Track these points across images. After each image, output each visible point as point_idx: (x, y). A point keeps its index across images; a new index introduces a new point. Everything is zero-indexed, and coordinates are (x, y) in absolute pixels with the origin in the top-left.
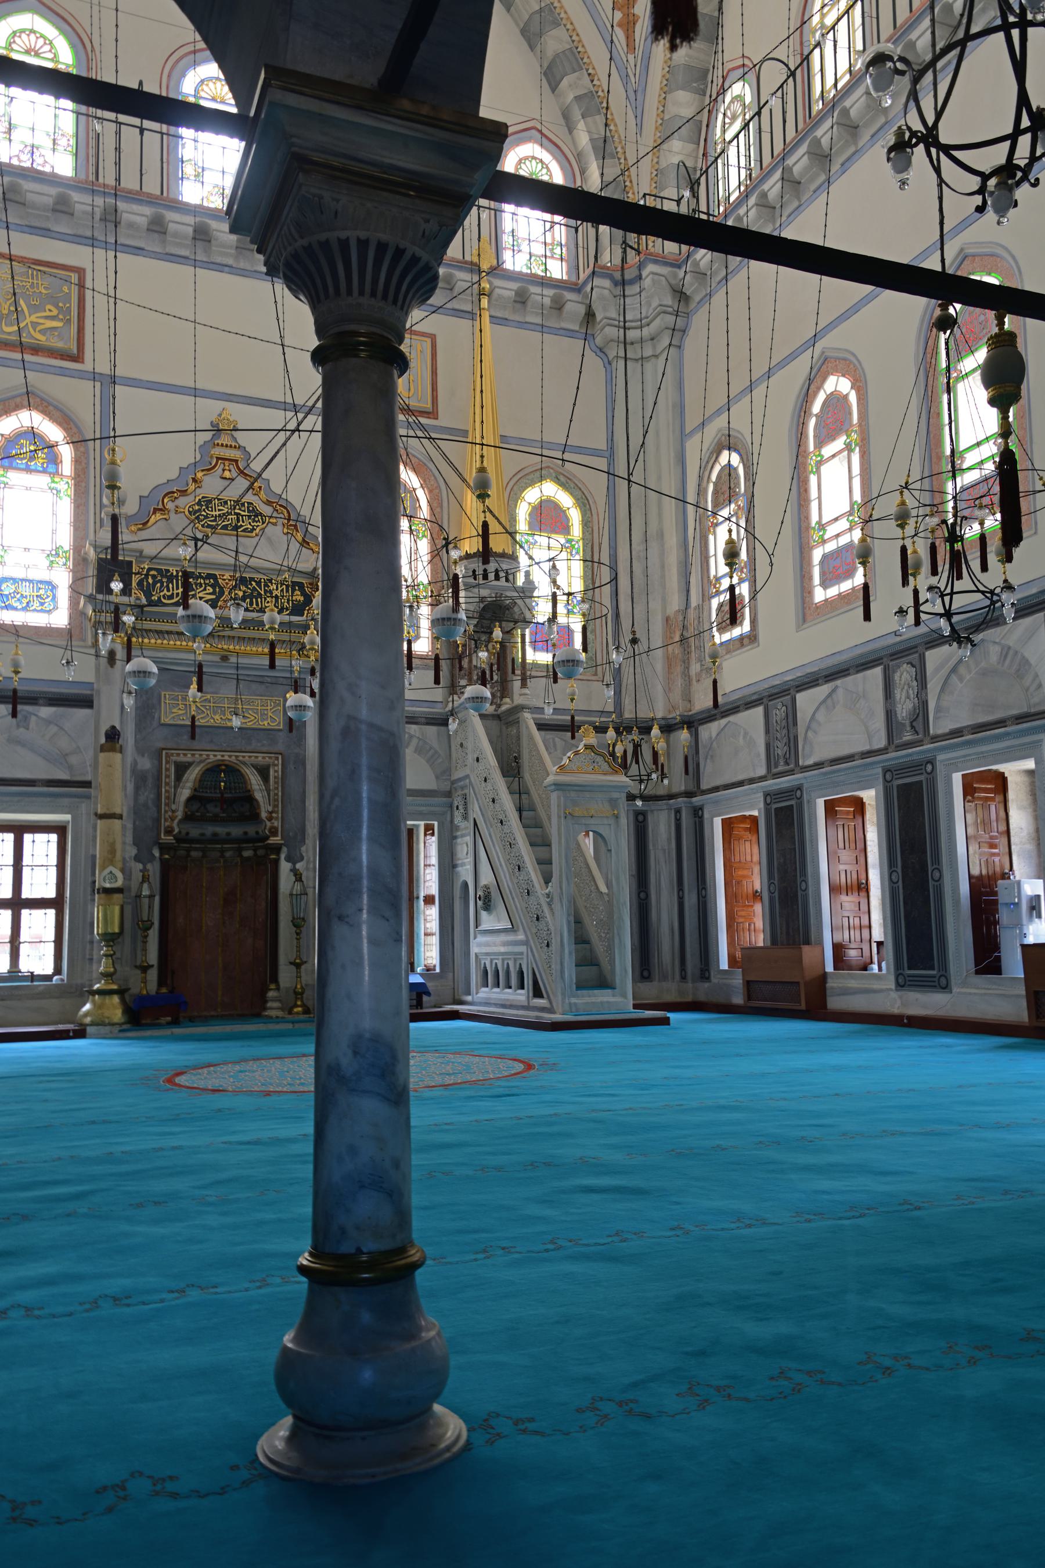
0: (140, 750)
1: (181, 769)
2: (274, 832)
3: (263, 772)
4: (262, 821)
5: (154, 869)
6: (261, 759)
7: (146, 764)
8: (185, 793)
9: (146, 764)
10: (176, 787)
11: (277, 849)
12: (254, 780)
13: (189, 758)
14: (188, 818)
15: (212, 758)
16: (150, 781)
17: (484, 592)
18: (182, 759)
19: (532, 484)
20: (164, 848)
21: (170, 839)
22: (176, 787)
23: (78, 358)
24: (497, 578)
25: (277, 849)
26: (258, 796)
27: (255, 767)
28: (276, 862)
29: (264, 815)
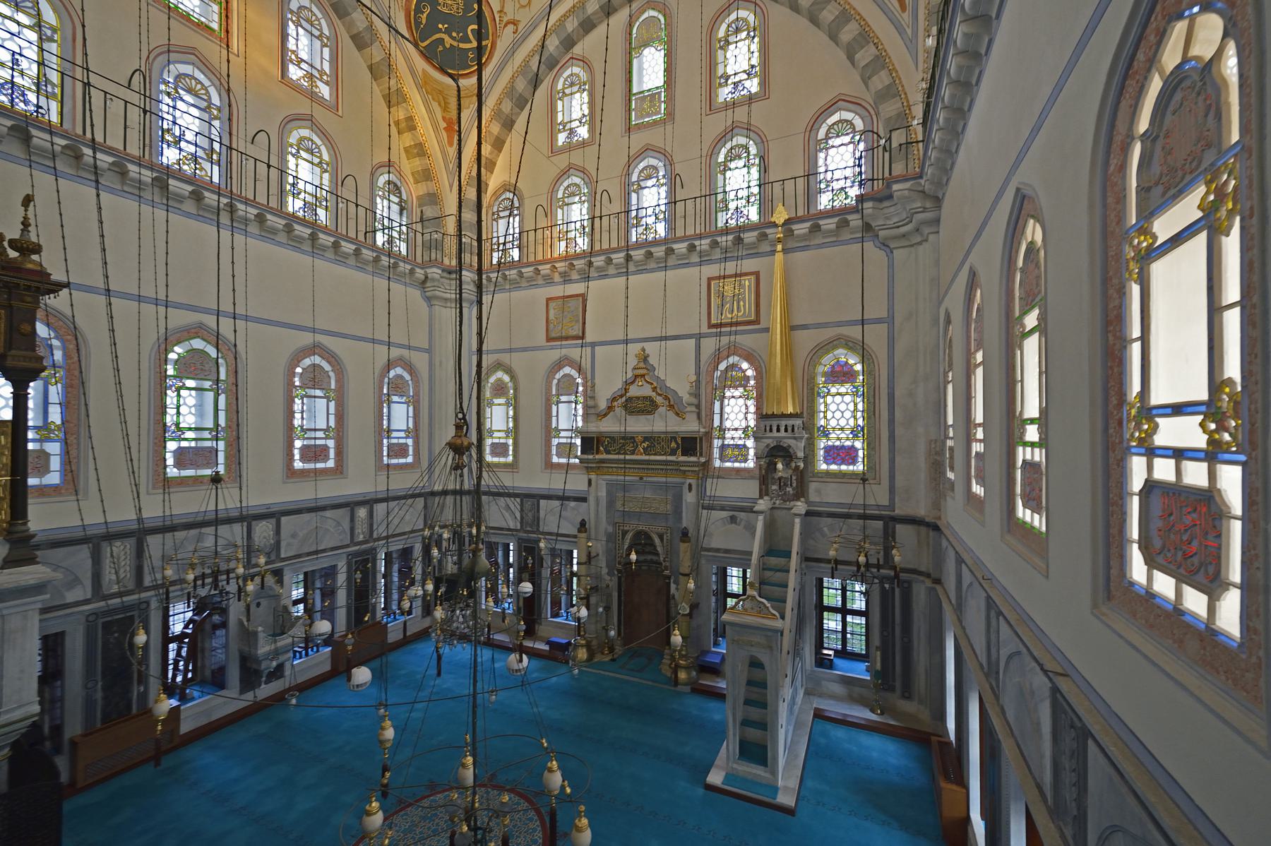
0: (608, 523)
1: (625, 533)
2: (666, 568)
5: (615, 579)
6: (660, 530)
7: (610, 529)
9: (610, 529)
11: (669, 578)
12: (657, 541)
17: (769, 441)
19: (827, 352)
20: (619, 571)
21: (620, 567)
23: (583, 337)
24: (778, 430)
26: (659, 549)
28: (669, 584)
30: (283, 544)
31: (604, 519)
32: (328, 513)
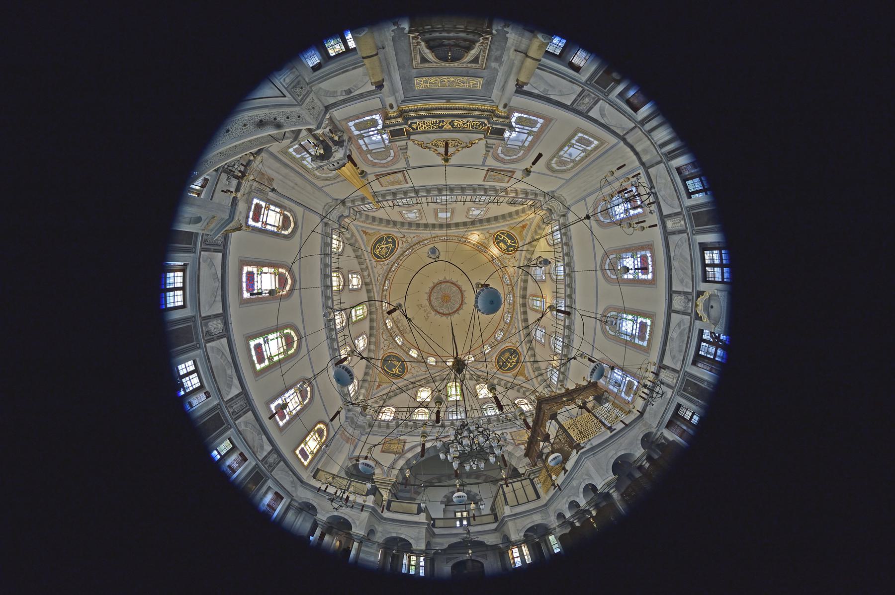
3: (424, 60)
4: (423, 40)
6: (426, 65)
8: (473, 52)
10: (479, 54)
12: (430, 55)
13: (469, 65)
14: (473, 42)
15: (456, 65)
16: (493, 58)
18: (474, 65)
22: (479, 54)
25: (410, 32)
26: (427, 51)
27: (429, 62)
29: (423, 44)
30: (686, 290)
31: (500, 74)
32: (672, 255)
